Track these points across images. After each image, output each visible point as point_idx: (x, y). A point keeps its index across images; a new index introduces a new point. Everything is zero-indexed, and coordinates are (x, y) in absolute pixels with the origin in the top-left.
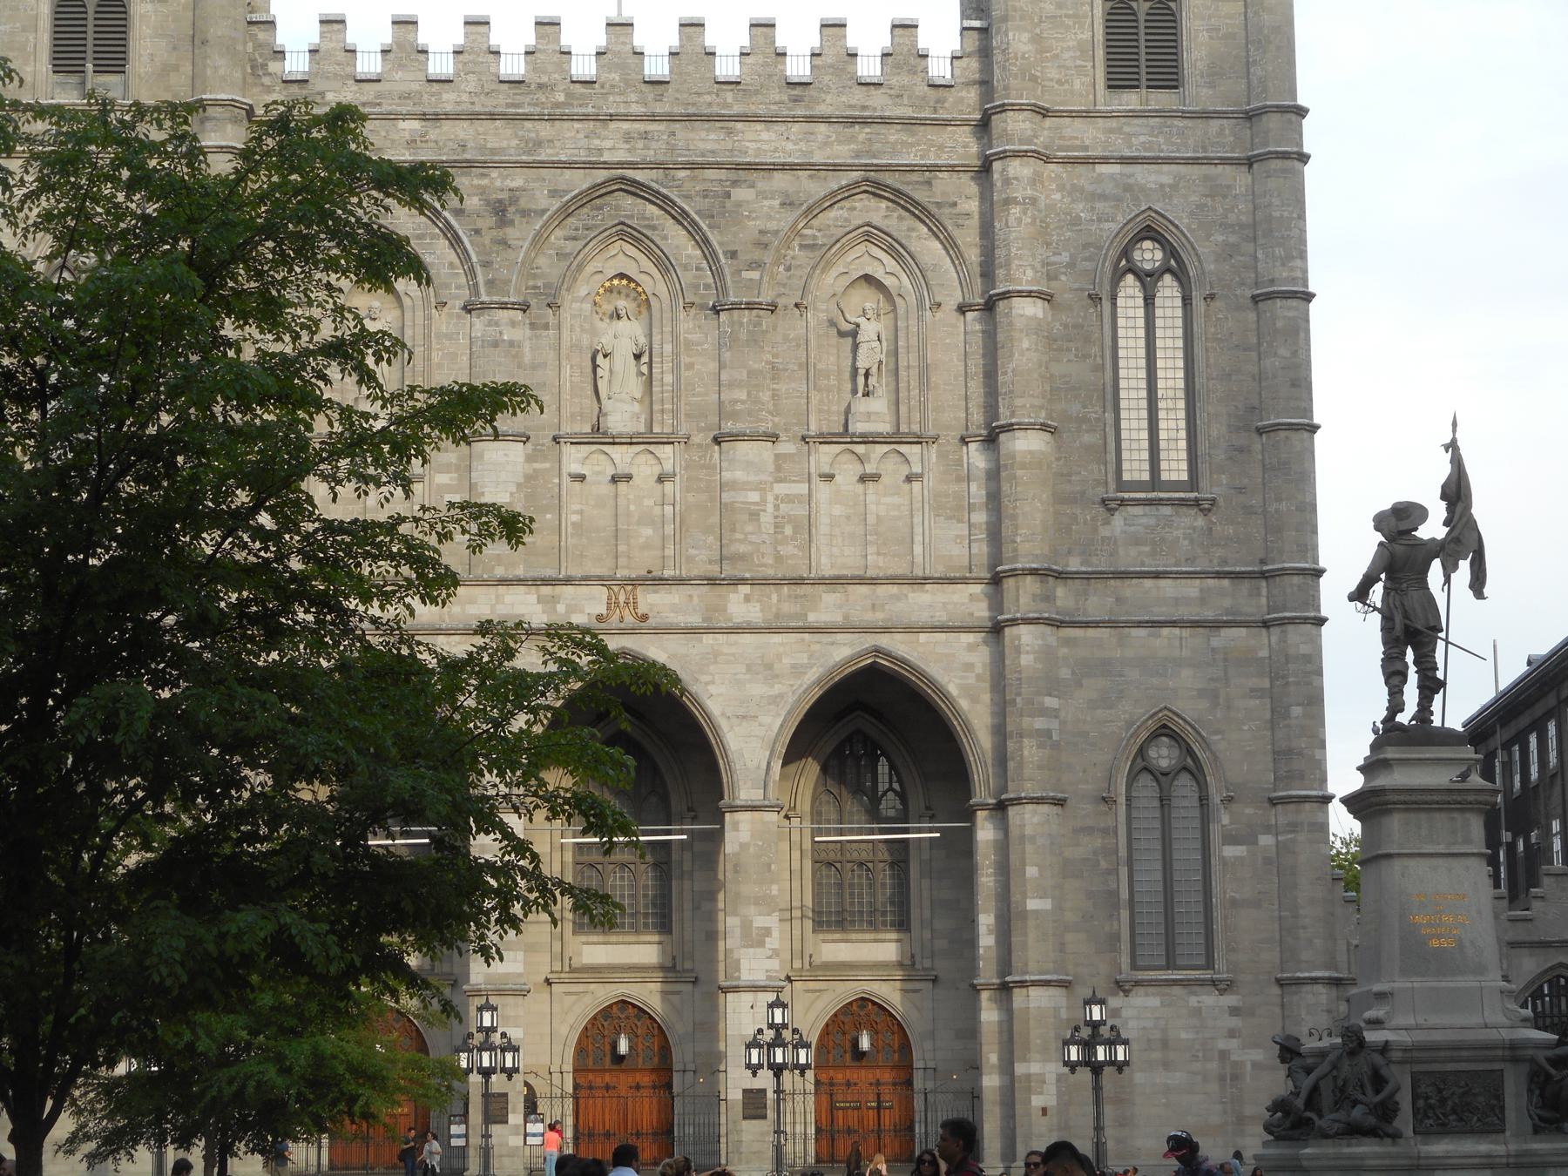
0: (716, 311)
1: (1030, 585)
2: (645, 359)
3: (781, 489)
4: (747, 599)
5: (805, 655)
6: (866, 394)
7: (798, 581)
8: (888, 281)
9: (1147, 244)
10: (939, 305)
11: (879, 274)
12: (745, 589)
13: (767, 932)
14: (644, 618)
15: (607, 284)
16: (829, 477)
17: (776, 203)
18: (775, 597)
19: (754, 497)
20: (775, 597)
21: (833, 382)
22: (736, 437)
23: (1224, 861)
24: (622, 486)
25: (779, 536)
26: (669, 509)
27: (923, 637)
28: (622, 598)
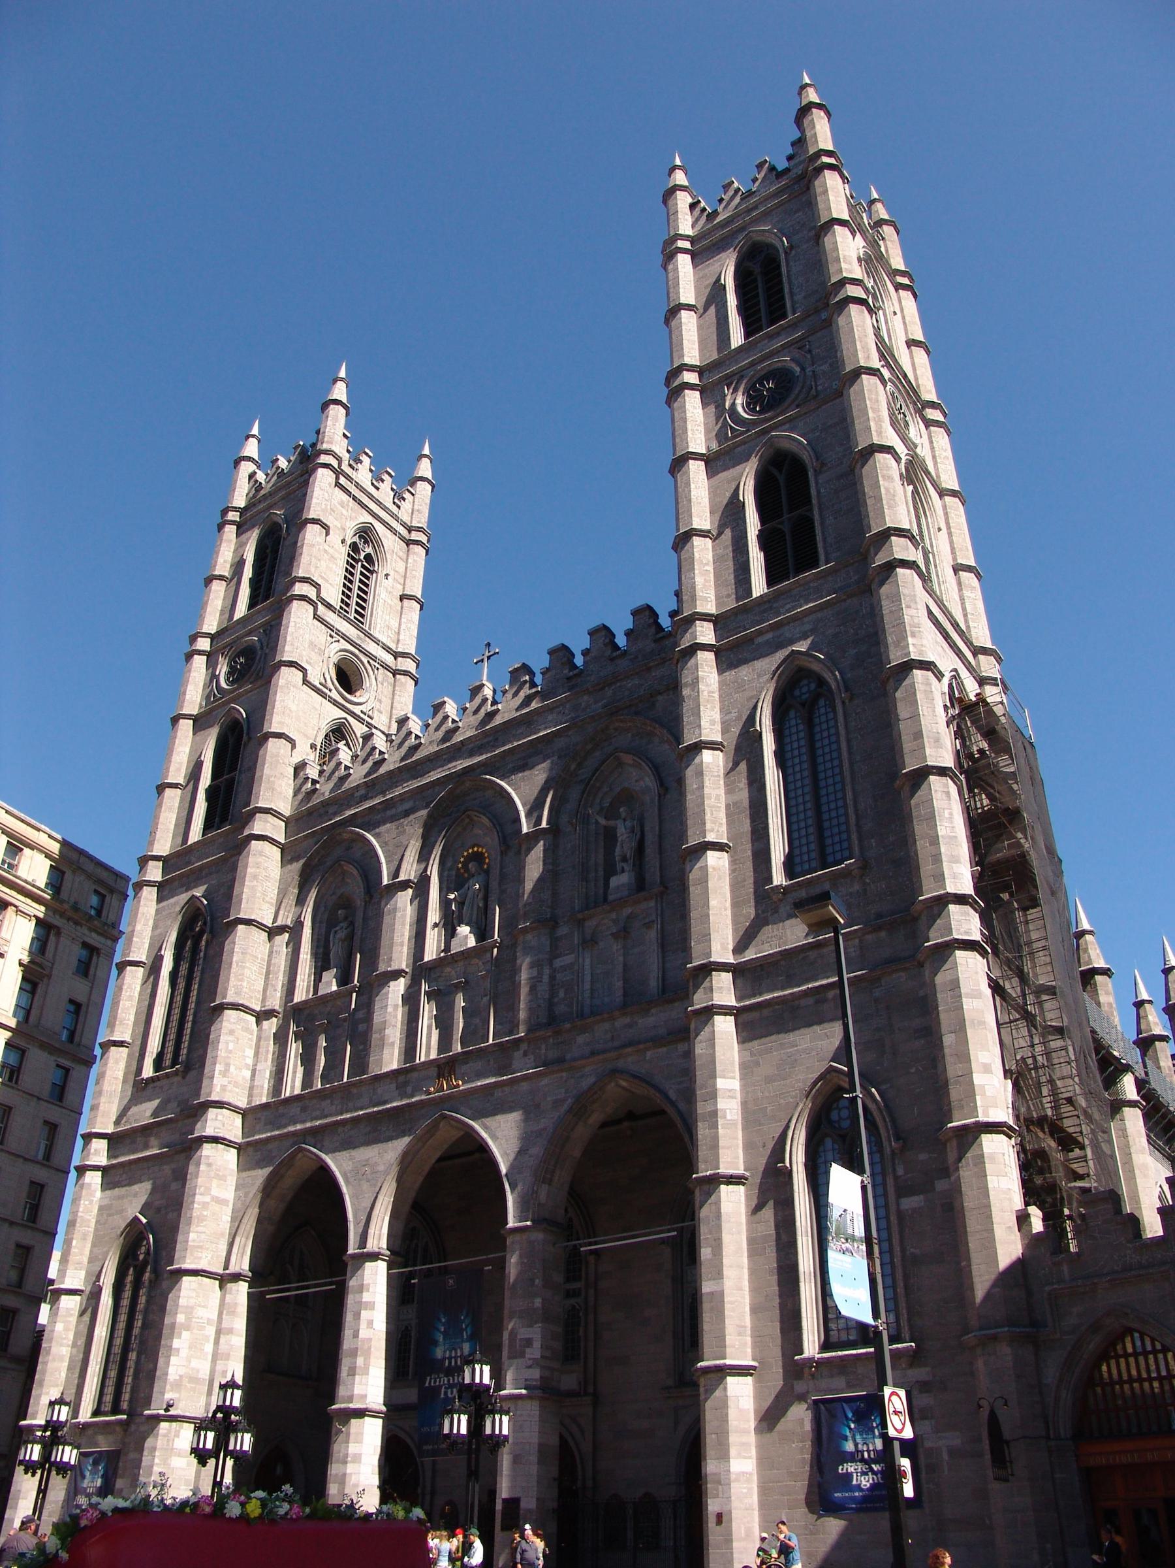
3: (558, 963)
4: (525, 1054)
5: (563, 1090)
6: (623, 871)
9: (805, 682)
10: (667, 790)
13: (529, 1342)
15: (465, 854)
16: (589, 942)
17: (555, 758)
18: (543, 1047)
20: (543, 1047)
21: (601, 873)
23: (901, 1216)
25: (556, 1000)
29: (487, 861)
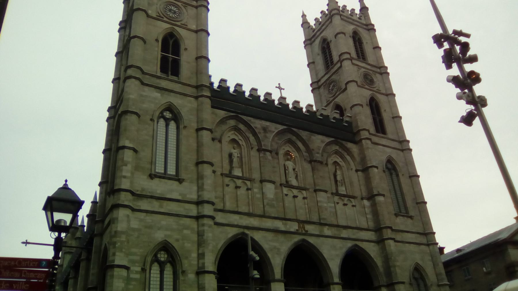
0: (310, 162)
1: (389, 231)
2: (296, 170)
7: (338, 226)
8: (340, 163)
11: (338, 161)
12: (327, 227)
14: (307, 231)
19: (325, 205)
22: (320, 190)
24: (296, 199)
26: (307, 206)
27: (364, 243)
28: (301, 226)
29: (293, 158)
